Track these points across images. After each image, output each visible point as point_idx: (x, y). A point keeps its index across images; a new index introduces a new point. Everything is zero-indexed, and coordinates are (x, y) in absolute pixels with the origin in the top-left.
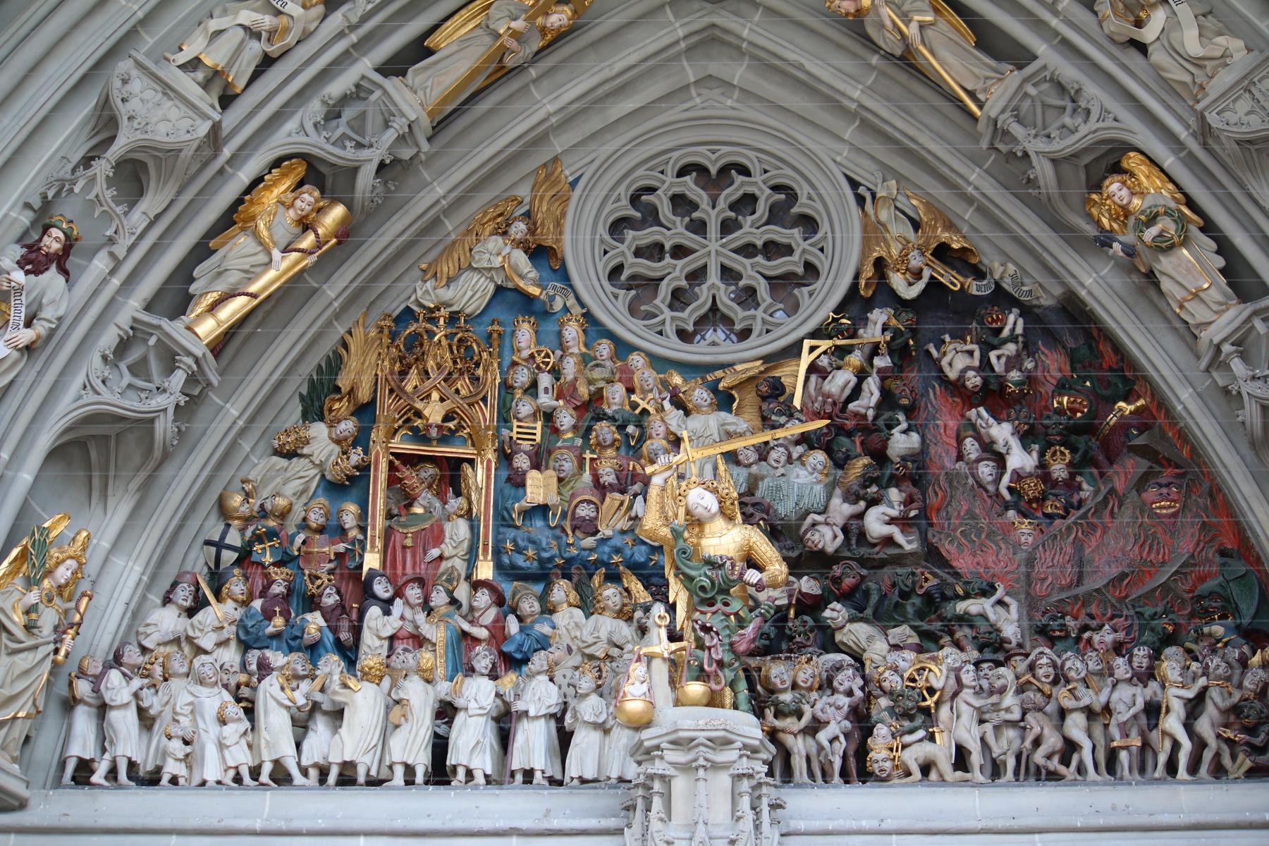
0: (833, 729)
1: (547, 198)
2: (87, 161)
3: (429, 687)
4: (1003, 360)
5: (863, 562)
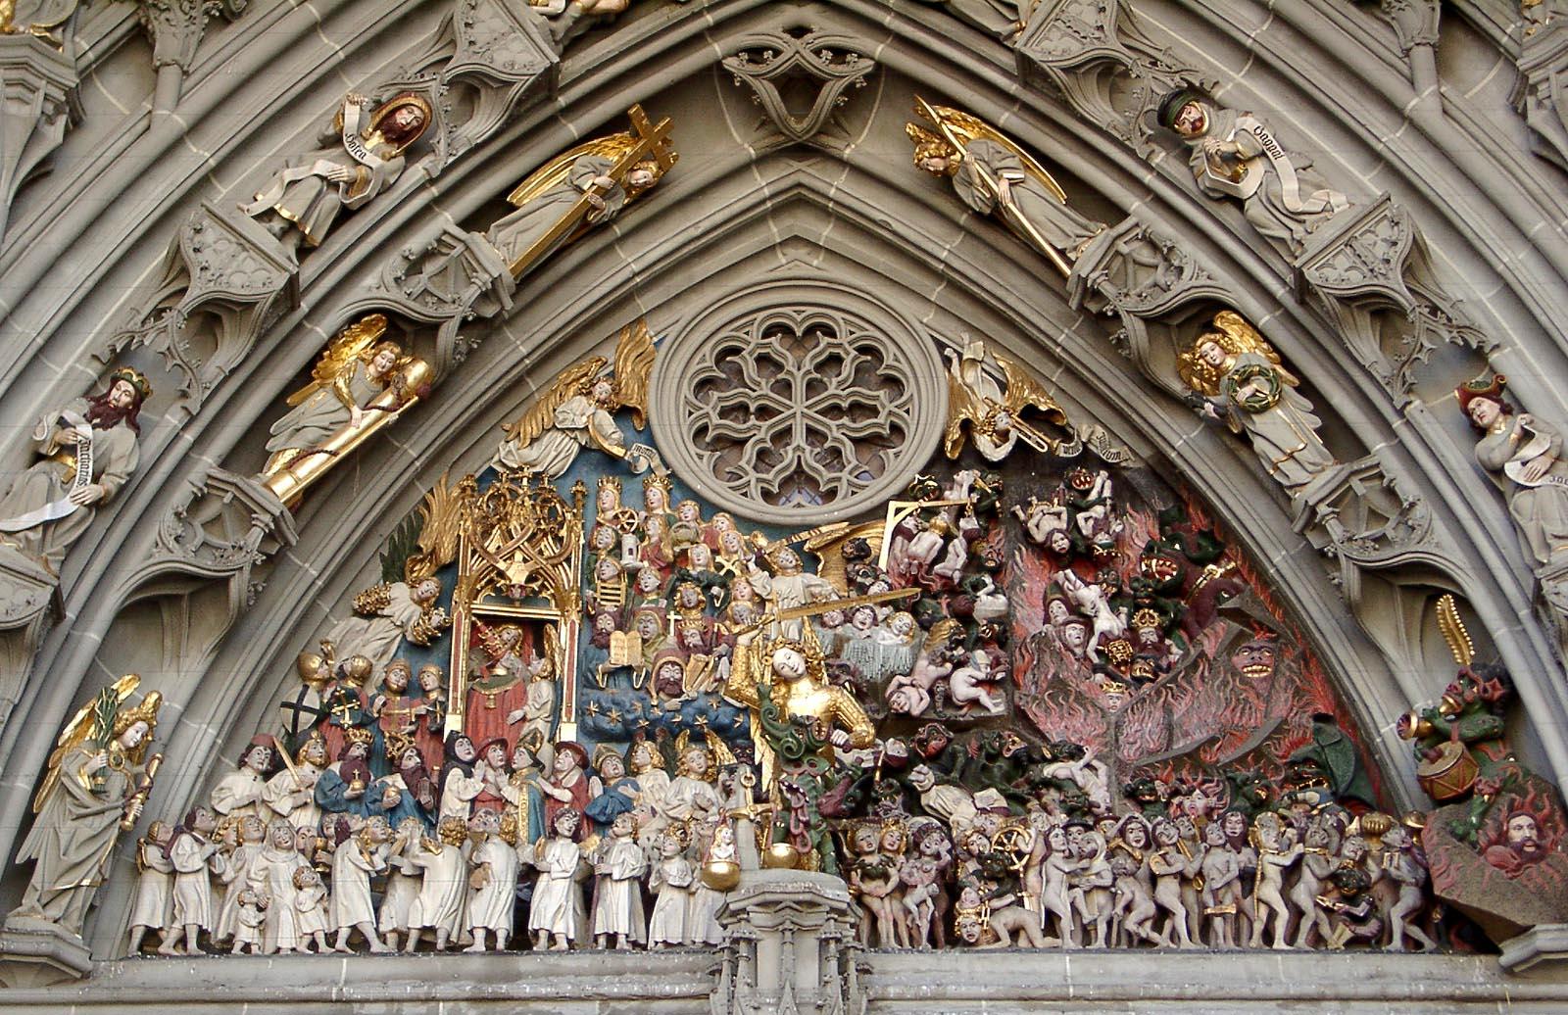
0: (920, 893)
1: (632, 358)
2: (158, 313)
3: (512, 850)
4: (1091, 522)
5: (954, 726)
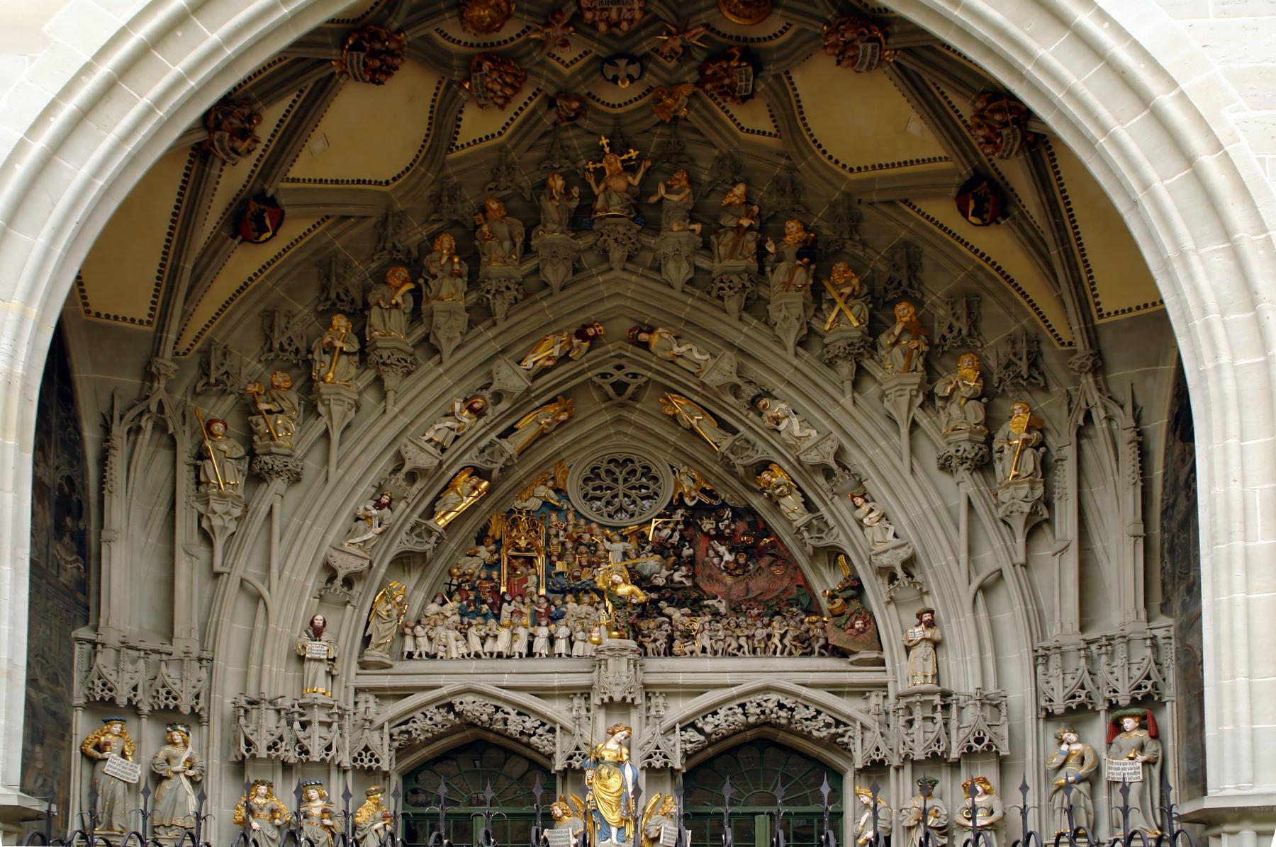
5: (672, 588)
